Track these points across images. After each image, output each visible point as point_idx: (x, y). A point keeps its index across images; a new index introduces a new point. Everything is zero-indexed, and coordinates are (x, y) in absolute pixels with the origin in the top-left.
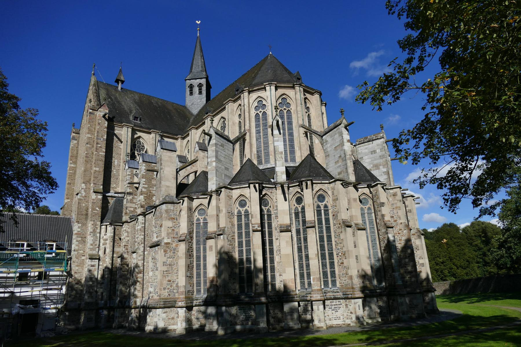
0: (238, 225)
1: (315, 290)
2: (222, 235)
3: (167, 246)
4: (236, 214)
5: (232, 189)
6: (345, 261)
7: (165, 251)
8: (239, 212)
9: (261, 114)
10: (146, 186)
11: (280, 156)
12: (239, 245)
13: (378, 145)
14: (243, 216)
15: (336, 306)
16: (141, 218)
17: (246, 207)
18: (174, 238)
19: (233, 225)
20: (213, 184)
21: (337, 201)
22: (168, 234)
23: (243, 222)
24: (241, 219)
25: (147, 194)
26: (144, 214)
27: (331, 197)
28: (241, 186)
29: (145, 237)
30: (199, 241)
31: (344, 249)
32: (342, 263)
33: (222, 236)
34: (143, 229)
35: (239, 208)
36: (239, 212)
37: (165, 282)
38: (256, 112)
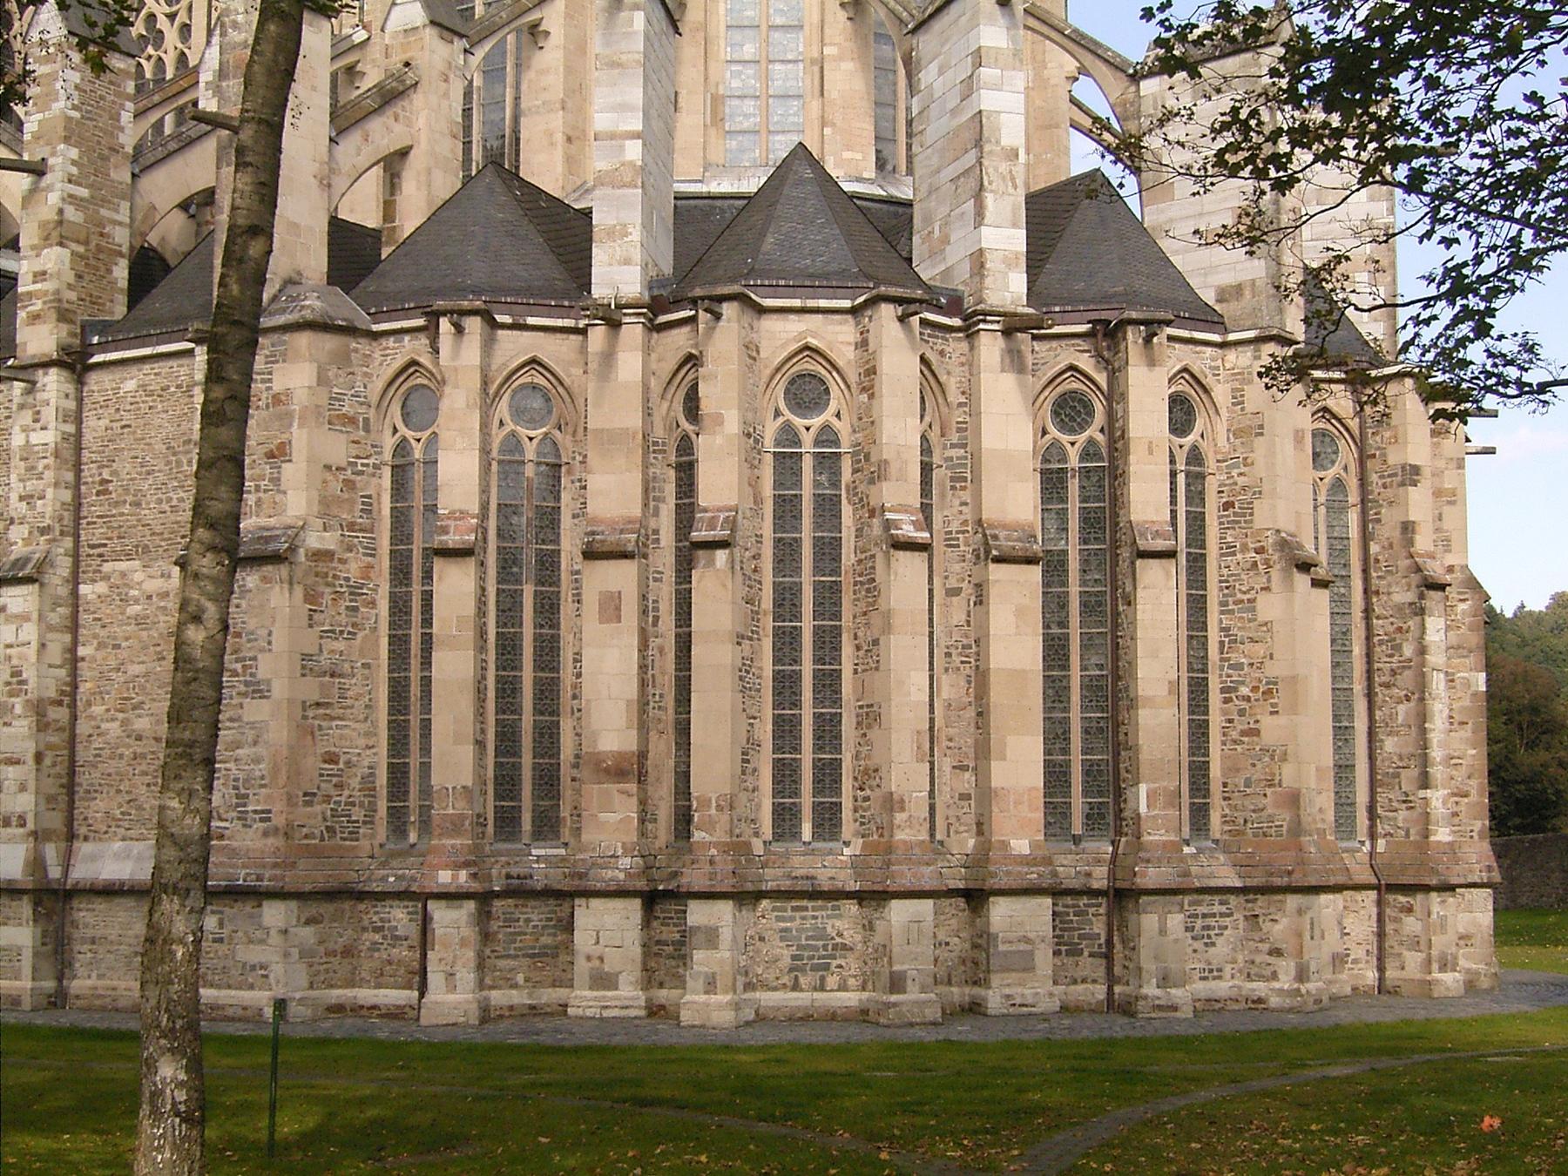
0: (780, 501)
2: (723, 544)
4: (769, 445)
5: (762, 311)
6: (1267, 723)
7: (311, 597)
8: (789, 435)
10: (83, 192)
12: (778, 604)
14: (807, 464)
16: (53, 383)
17: (827, 416)
18: (352, 526)
19: (758, 500)
20: (627, 262)
23: (807, 491)
24: (798, 473)
26: (75, 362)
29: (78, 496)
30: (516, 562)
33: (721, 556)
34: (68, 454)
35: (788, 415)
36: (789, 435)
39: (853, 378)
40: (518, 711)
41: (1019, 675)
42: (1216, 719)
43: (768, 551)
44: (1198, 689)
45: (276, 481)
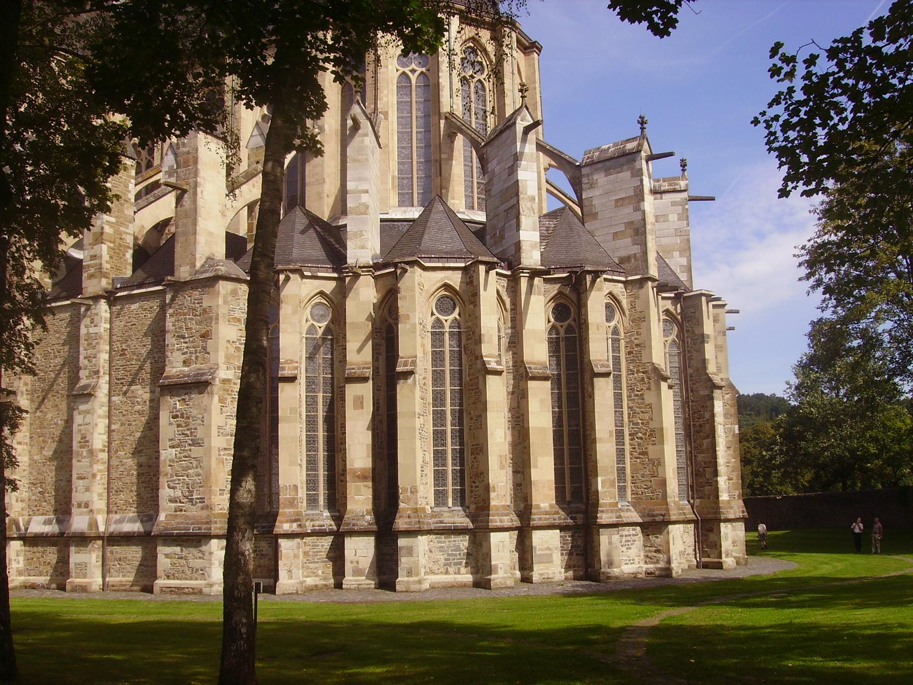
1: (605, 505)
3: (227, 386)
9: (413, 78)
11: (529, 204)
12: (434, 399)
13: (674, 204)
14: (447, 336)
15: (628, 538)
21: (643, 325)
22: (228, 357)
24: (442, 341)
25: (114, 242)
27: (627, 313)
28: (447, 265)
31: (653, 425)
32: (645, 453)
36: (438, 323)
37: (222, 475)
38: (401, 70)
39: (465, 298)
40: (316, 450)
41: (543, 429)
42: (627, 448)
43: (430, 376)
44: (620, 435)
45: (205, 348)
